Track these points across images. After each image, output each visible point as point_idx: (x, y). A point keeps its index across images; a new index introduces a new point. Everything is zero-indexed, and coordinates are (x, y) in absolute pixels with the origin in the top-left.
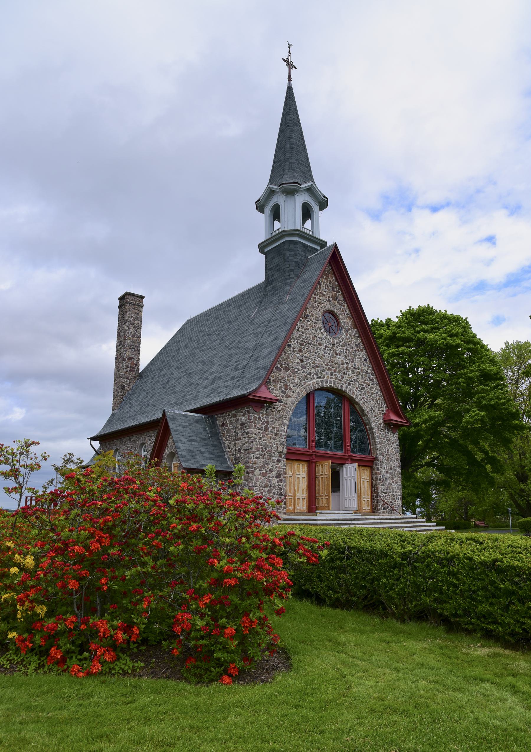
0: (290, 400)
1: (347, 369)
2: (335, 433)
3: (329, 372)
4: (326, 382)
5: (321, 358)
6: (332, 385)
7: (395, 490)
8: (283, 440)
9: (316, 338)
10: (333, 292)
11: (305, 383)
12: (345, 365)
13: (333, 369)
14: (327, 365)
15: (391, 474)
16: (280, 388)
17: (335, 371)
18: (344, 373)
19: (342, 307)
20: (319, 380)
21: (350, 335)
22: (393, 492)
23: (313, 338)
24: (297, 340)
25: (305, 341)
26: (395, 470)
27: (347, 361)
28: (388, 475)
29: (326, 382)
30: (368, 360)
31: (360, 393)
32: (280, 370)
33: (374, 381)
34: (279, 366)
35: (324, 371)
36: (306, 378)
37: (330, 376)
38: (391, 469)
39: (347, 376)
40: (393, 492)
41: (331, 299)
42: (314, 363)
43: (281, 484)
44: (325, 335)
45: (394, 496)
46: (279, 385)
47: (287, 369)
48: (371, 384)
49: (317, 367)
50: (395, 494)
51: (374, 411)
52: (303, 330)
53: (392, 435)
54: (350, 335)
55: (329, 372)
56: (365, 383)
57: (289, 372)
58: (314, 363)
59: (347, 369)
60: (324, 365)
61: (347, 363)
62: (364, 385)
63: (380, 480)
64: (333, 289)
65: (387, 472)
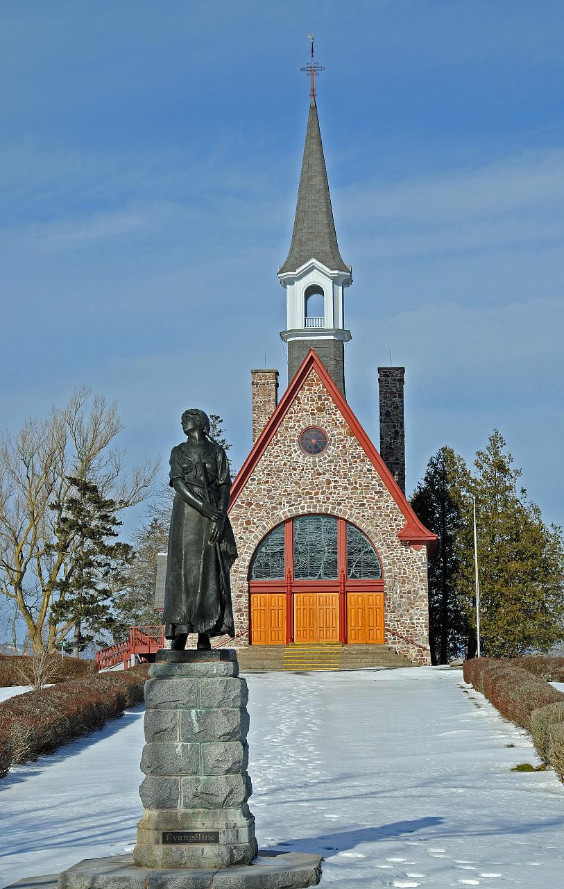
0: (253, 534)
1: (335, 487)
2: (326, 559)
3: (308, 497)
4: (303, 508)
5: (296, 483)
6: (311, 510)
7: (415, 617)
8: (244, 576)
9: (289, 463)
10: (319, 403)
11: (273, 515)
12: (333, 484)
13: (313, 492)
14: (304, 489)
15: (409, 598)
16: (242, 524)
17: (317, 494)
18: (331, 493)
19: (334, 417)
20: (293, 508)
21: (344, 447)
22: (411, 619)
23: (285, 464)
24: (263, 471)
25: (274, 469)
26: (417, 594)
27: (337, 478)
28: (404, 600)
29: (303, 508)
30: (373, 469)
31: (357, 511)
32: (241, 507)
33: (382, 493)
34: (240, 503)
35: (300, 497)
36: (275, 508)
37: (308, 501)
38: (409, 592)
39: (335, 496)
40: (411, 619)
41: (316, 411)
42: (286, 491)
43: (242, 618)
44: (301, 457)
45: (413, 624)
46: (239, 522)
47: (249, 504)
48: (376, 497)
49: (290, 494)
50: (415, 621)
51: (381, 528)
52: (272, 458)
53: (415, 552)
54: (344, 447)
55: (308, 497)
56: (366, 498)
57: (253, 506)
58: (286, 491)
59: (335, 487)
60: (299, 490)
61: (336, 481)
62: (365, 500)
63: (389, 606)
64: (320, 398)
65: (401, 597)
